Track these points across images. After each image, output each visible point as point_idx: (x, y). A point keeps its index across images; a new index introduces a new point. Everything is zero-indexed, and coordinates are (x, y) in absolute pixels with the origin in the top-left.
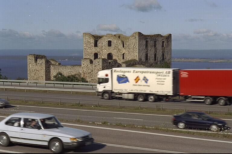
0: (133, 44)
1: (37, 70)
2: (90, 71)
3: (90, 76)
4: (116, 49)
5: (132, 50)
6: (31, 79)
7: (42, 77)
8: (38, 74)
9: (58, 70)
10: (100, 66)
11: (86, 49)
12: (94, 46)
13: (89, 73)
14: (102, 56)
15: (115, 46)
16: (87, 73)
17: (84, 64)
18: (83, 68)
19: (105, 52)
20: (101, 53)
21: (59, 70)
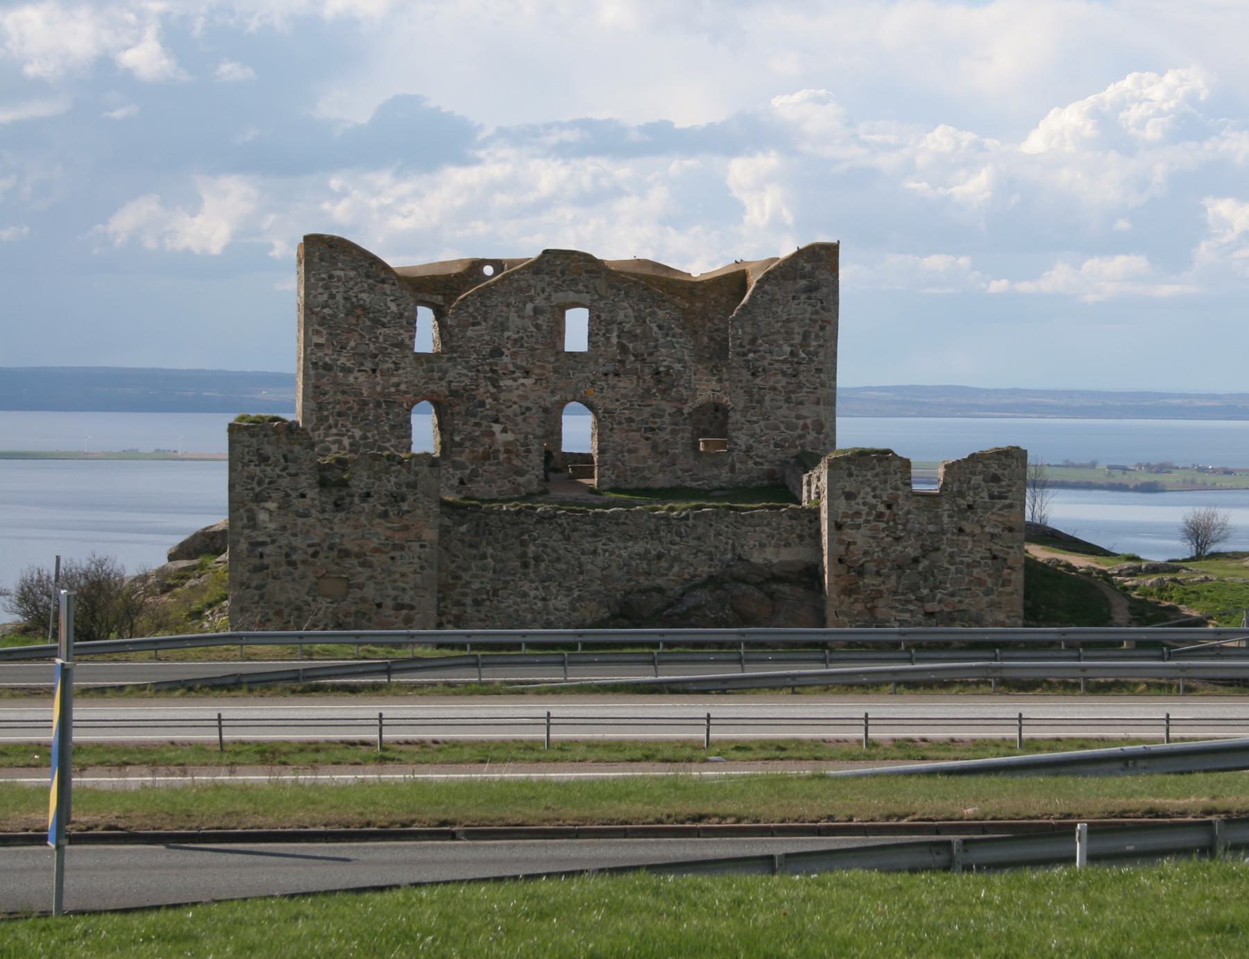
0: (789, 333)
1: (345, 553)
2: (912, 552)
3: (914, 588)
4: (634, 371)
5: (782, 382)
7: (399, 607)
10: (1011, 506)
11: (327, 367)
14: (497, 428)
15: (623, 349)
16: (880, 562)
19: (524, 397)
20: (482, 404)
21: (524, 544)
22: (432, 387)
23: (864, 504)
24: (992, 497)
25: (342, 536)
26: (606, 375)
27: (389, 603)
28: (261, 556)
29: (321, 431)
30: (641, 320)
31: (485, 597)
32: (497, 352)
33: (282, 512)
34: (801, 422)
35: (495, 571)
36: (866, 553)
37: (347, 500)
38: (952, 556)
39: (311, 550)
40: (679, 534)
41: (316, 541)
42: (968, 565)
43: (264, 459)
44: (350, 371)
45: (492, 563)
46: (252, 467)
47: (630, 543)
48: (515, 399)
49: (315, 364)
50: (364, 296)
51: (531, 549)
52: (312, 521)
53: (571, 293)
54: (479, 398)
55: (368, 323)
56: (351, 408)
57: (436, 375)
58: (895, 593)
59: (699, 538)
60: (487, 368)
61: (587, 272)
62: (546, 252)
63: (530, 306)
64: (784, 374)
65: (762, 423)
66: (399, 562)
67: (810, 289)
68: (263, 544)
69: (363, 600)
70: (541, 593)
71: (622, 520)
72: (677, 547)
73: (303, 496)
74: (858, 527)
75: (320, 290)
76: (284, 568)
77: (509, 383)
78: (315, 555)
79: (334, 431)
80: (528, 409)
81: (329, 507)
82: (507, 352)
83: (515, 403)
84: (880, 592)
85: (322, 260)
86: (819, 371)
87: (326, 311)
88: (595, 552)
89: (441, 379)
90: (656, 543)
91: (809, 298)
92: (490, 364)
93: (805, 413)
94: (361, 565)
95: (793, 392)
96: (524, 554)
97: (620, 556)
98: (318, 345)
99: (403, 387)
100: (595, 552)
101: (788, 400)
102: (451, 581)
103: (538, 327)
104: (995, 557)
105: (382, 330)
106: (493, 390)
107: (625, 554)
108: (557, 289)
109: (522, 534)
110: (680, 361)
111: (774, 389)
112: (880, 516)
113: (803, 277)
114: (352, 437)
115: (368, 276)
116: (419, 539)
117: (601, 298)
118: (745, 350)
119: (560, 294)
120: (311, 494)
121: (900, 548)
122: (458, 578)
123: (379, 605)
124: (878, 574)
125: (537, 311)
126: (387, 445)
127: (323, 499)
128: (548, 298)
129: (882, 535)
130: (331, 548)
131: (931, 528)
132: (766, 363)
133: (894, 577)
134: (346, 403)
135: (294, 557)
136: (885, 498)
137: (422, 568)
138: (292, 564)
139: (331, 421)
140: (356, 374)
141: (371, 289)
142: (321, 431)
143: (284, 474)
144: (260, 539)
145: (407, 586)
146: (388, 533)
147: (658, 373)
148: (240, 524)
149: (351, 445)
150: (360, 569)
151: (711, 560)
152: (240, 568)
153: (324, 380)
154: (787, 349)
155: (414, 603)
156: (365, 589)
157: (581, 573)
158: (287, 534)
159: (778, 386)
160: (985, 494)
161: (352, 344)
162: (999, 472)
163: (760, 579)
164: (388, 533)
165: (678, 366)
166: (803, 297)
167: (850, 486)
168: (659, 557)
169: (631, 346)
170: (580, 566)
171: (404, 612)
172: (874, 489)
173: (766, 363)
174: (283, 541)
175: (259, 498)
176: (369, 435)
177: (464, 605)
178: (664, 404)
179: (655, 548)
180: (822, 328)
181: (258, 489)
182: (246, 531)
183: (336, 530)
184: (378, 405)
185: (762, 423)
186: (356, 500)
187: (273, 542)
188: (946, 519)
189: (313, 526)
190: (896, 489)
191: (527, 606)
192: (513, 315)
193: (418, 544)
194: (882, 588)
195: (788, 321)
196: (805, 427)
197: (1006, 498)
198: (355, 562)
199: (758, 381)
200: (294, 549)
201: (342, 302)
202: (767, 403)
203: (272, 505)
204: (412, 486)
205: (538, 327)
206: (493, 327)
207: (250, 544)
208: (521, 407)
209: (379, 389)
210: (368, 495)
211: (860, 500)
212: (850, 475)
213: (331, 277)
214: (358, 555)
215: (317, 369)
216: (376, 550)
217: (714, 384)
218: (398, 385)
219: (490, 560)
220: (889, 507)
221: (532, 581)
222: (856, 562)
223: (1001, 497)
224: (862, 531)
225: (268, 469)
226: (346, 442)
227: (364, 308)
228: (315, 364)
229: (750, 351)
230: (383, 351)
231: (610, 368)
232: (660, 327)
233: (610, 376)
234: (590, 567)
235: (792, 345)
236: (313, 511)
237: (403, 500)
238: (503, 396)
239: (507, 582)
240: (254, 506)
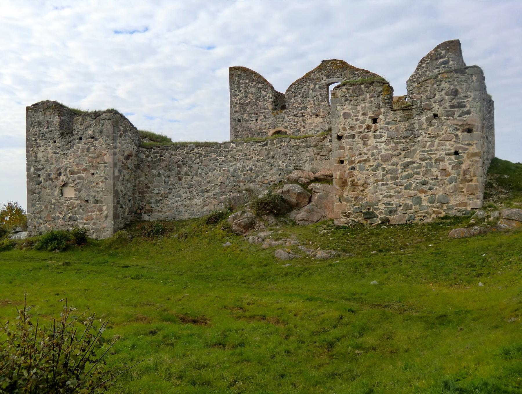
6: (43, 215)
7: (97, 202)
10: (468, 113)
11: (239, 121)
12: (270, 107)
18: (340, 138)
19: (316, 126)
20: (299, 130)
24: (452, 107)
27: (91, 200)
28: (39, 176)
31: (161, 198)
35: (165, 182)
43: (40, 124)
45: (164, 178)
52: (59, 155)
53: (334, 78)
59: (273, 157)
61: (340, 68)
66: (95, 176)
70: (188, 195)
73: (55, 142)
80: (318, 131)
83: (312, 129)
96: (179, 173)
97: (229, 171)
98: (236, 112)
99: (268, 126)
102: (145, 190)
103: (320, 95)
106: (303, 124)
107: (232, 169)
113: (441, 58)
116: (104, 163)
120: (58, 141)
122: (149, 187)
123: (87, 201)
125: (320, 88)
134: (246, 134)
136: (370, 114)
137: (106, 179)
138: (51, 179)
144: (39, 167)
146: (90, 159)
153: (238, 126)
155: (102, 200)
156: (81, 192)
161: (248, 110)
164: (90, 159)
171: (98, 205)
177: (151, 203)
184: (258, 134)
187: (44, 168)
191: (181, 203)
193: (103, 165)
197: (465, 106)
201: (244, 93)
206: (302, 97)
208: (315, 131)
213: (239, 83)
215: (236, 122)
218: (266, 125)
219: (163, 176)
221: (184, 188)
223: (460, 106)
224: (356, 138)
228: (234, 119)
239: (170, 189)
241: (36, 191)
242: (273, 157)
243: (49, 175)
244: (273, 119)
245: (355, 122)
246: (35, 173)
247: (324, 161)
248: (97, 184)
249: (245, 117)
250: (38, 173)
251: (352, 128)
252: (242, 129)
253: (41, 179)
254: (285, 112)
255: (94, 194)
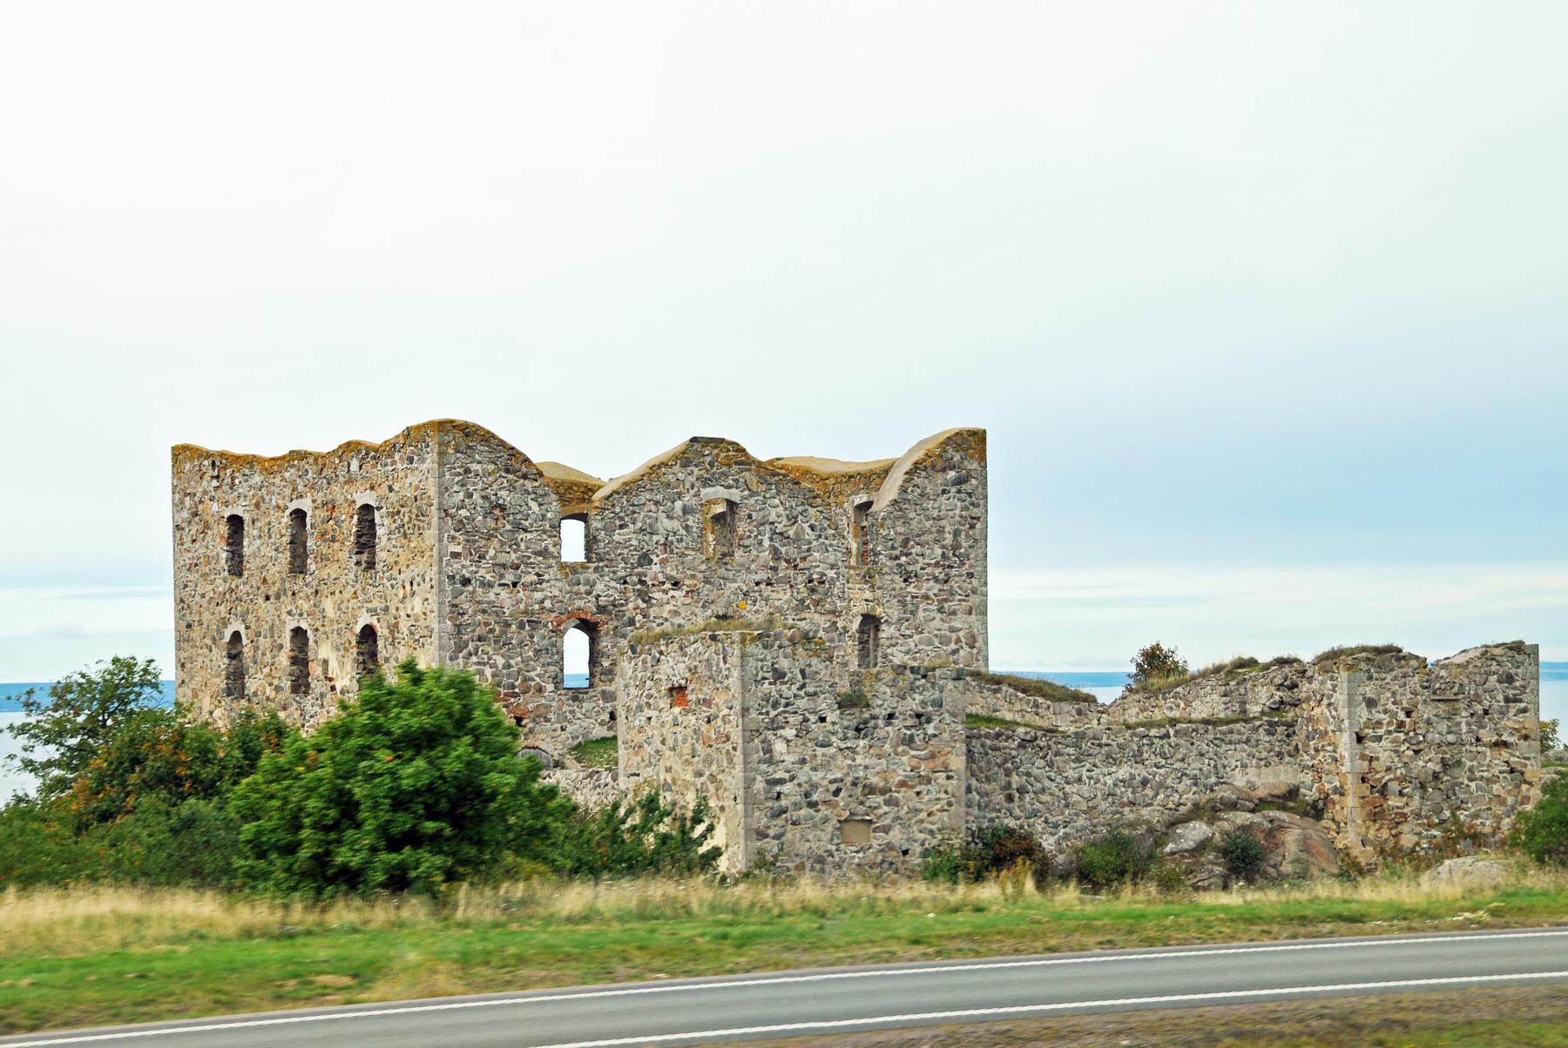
0: (941, 531)
1: (871, 790)
2: (1434, 766)
3: (1439, 812)
8: (886, 829)
9: (1003, 779)
10: (1525, 711)
11: (466, 582)
13: (1423, 786)
17: (1371, 703)
19: (676, 613)
20: (632, 622)
22: (579, 603)
23: (1385, 712)
24: (1507, 700)
25: (866, 767)
26: (757, 584)
29: (460, 660)
30: (793, 520)
32: (645, 559)
33: (800, 741)
34: (954, 636)
36: (1388, 769)
37: (872, 723)
38: (1471, 770)
39: (833, 787)
40: (1163, 755)
41: (839, 775)
42: (1488, 781)
43: (779, 675)
44: (490, 585)
46: (766, 685)
47: (1114, 769)
48: (665, 615)
49: (451, 578)
50: (504, 493)
51: (1016, 780)
52: (832, 750)
54: (628, 614)
55: (508, 527)
56: (492, 631)
57: (582, 589)
58: (1418, 816)
59: (1183, 760)
60: (635, 579)
62: (694, 440)
63: (678, 504)
64: (936, 579)
65: (916, 637)
67: (959, 481)
68: (781, 782)
69: (890, 847)
71: (1104, 741)
72: (1162, 771)
73: (823, 720)
74: (1379, 739)
75: (456, 488)
76: (805, 812)
77: (657, 595)
78: (837, 792)
79: (474, 659)
81: (851, 733)
82: (655, 559)
84: (1404, 815)
85: (457, 451)
86: (970, 575)
87: (463, 513)
88: (1080, 780)
89: (588, 593)
90: (1140, 766)
91: (959, 491)
92: (639, 574)
93: (958, 625)
94: (887, 803)
95: (946, 600)
96: (1009, 785)
98: (455, 555)
99: (548, 604)
100: (1080, 780)
101: (940, 610)
103: (687, 528)
104: (1512, 771)
105: (523, 535)
108: (706, 482)
109: (1006, 761)
110: (832, 567)
111: (926, 597)
112: (1401, 725)
114: (494, 666)
115: (507, 471)
116: (946, 769)
117: (753, 494)
118: (897, 552)
119: (709, 490)
121: (1421, 763)
123: (905, 853)
124: (1401, 794)
125: (686, 510)
126: (532, 674)
127: (846, 723)
128: (697, 495)
129: (1403, 748)
130: (854, 784)
131: (1451, 738)
132: (918, 567)
133: (1417, 797)
134: (487, 624)
135: (815, 797)
136: (1405, 704)
137: (950, 804)
138: (813, 805)
139: (471, 647)
140: (497, 589)
141: (512, 488)
142: (460, 660)
143: (802, 693)
144: (777, 776)
145: (934, 827)
146: (914, 762)
147: (811, 581)
148: (755, 757)
149: (494, 675)
150: (886, 809)
151: (1196, 784)
152: (757, 813)
154: (939, 552)
157: (1067, 806)
158: (807, 768)
159: (931, 594)
160: (1500, 697)
161: (492, 552)
162: (1513, 671)
163: (1252, 806)
165: (831, 574)
166: (953, 489)
167: (1369, 690)
168: (1144, 783)
169: (783, 550)
170: (1066, 797)
172: (1394, 694)
173: (918, 567)
174: (802, 778)
175: (774, 726)
176: (512, 662)
178: (817, 616)
179: (1141, 772)
180: (972, 527)
181: (773, 713)
182: (764, 767)
183: (859, 761)
184: (521, 626)
185: (916, 637)
186: (880, 722)
187: (792, 778)
188: (1464, 728)
189: (833, 757)
190: (1415, 693)
192: (662, 516)
193: (944, 775)
194: (1406, 810)
195: (939, 518)
196: (958, 641)
198: (880, 799)
199: (910, 589)
200: (815, 786)
202: (921, 614)
203: (789, 733)
204: (938, 704)
205: (687, 528)
207: (768, 782)
209: (522, 606)
210: (891, 716)
211: (1380, 708)
212: (1370, 678)
213: (467, 471)
214: (883, 791)
216: (903, 784)
217: (868, 595)
220: (1408, 714)
222: (1379, 780)
224: (1383, 743)
225: (784, 687)
226: (488, 671)
227: (503, 508)
228: (451, 578)
229: (902, 554)
230: (524, 560)
231: (762, 575)
232: (812, 528)
233: (763, 586)
234: (1076, 798)
235: (943, 547)
236: (834, 739)
237: (928, 722)
238: (652, 612)
240: (769, 735)
241: (771, 832)
242: (1183, 760)
243: (807, 795)
244: (560, 584)
245: (1382, 716)
246: (767, 792)
247: (1264, 770)
248: (929, 815)
249: (482, 572)
250: (778, 788)
251: (1379, 723)
252: (474, 607)
253: (784, 802)
254: (596, 569)
255: (922, 836)
